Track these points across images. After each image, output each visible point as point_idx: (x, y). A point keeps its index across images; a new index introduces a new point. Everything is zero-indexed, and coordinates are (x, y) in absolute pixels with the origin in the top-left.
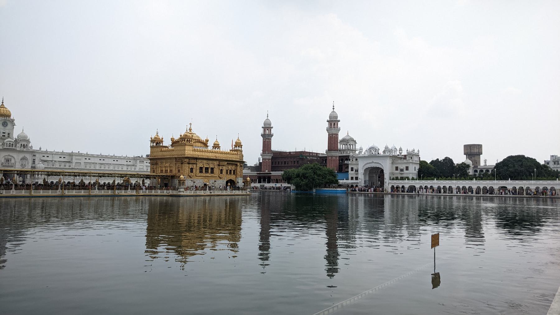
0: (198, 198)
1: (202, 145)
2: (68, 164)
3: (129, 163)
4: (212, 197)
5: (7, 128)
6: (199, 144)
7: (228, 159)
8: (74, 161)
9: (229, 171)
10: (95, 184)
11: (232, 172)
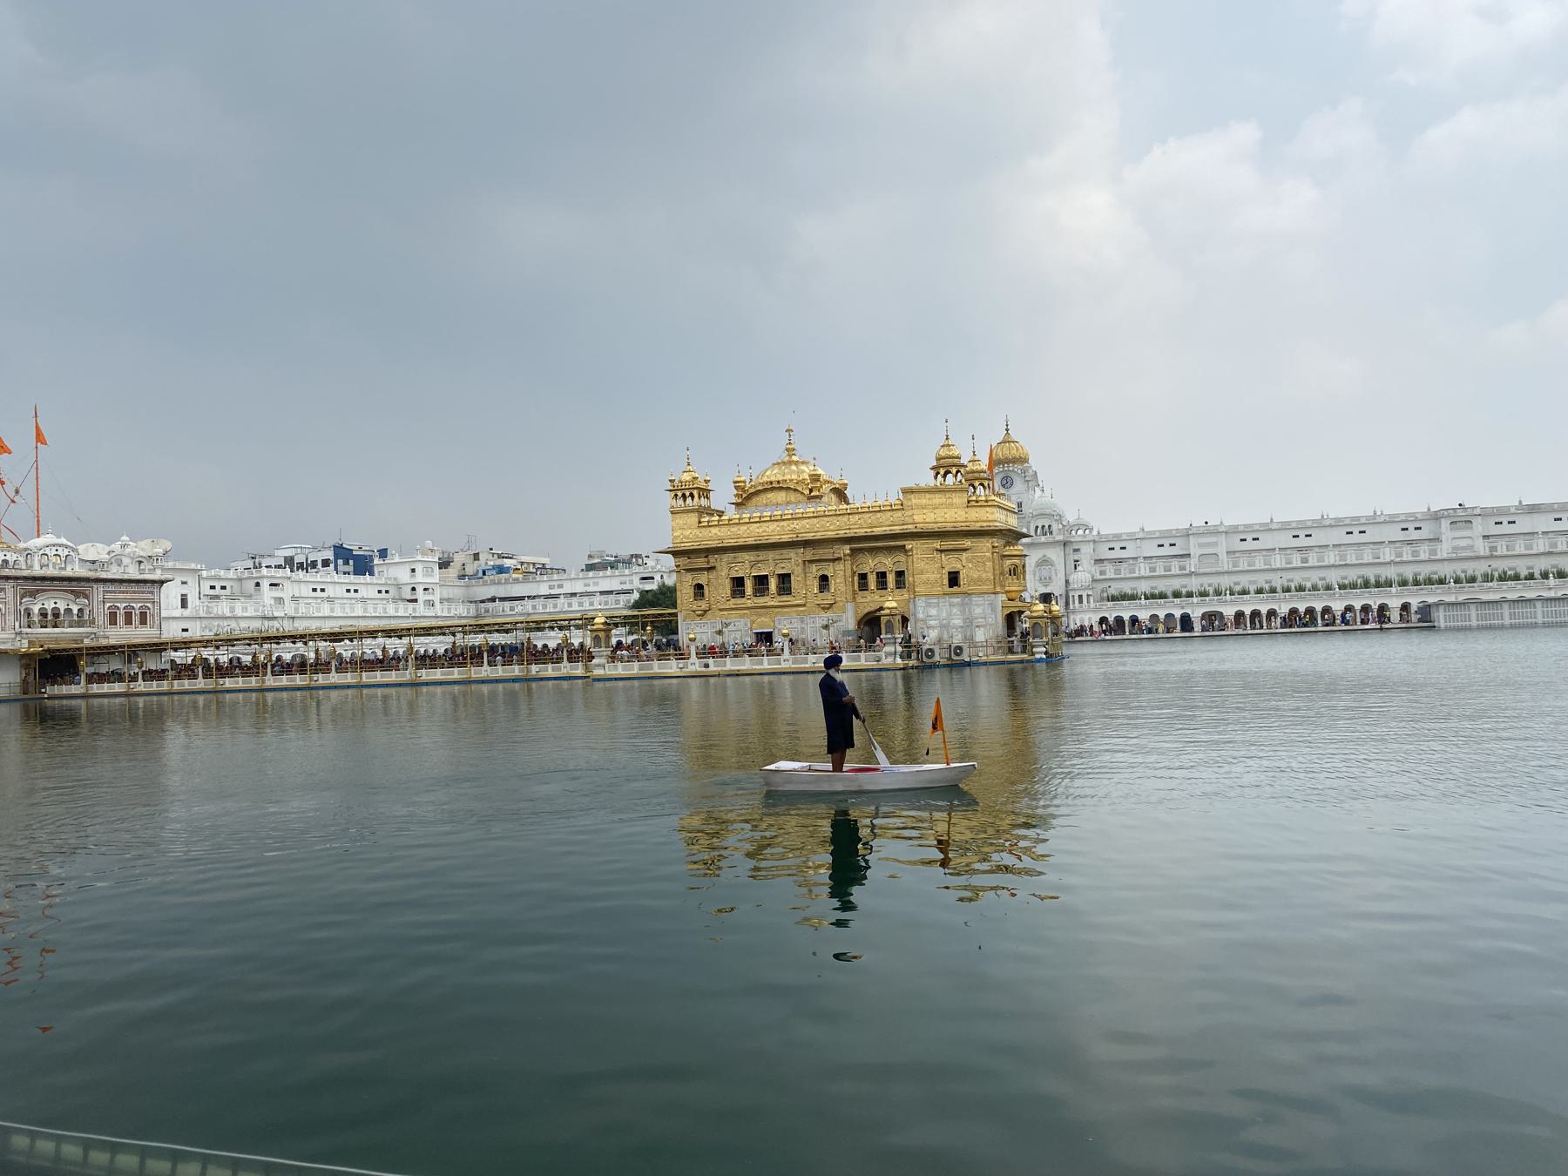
0: (656, 682)
1: (792, 496)
2: (1175, 563)
3: (1415, 535)
4: (712, 680)
5: (1013, 490)
6: (781, 496)
7: (851, 533)
8: (1195, 551)
9: (872, 581)
10: (558, 649)
11: (891, 578)
